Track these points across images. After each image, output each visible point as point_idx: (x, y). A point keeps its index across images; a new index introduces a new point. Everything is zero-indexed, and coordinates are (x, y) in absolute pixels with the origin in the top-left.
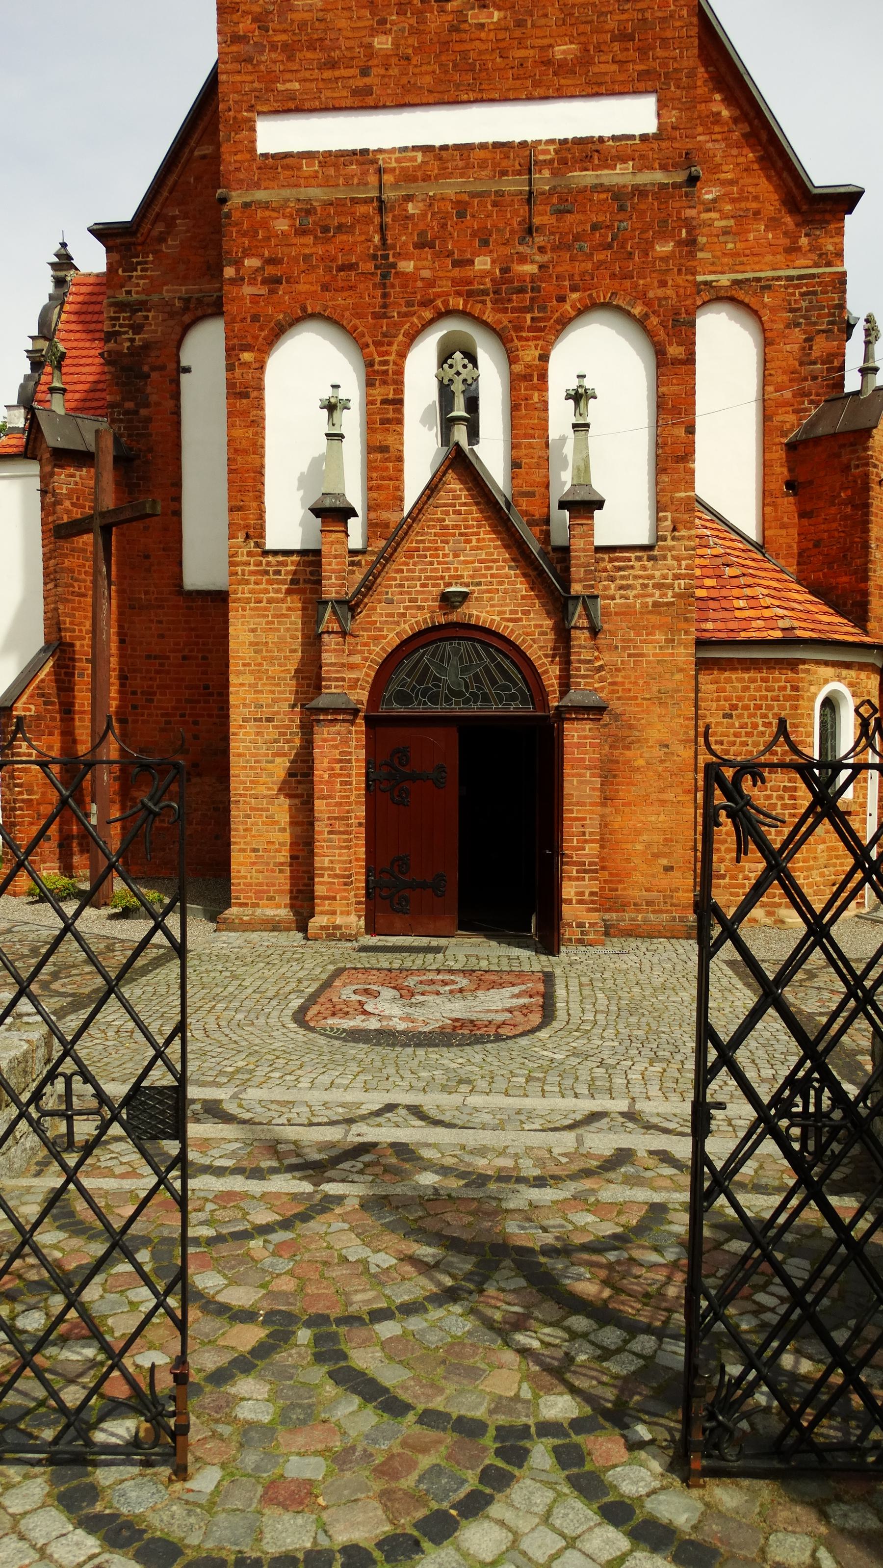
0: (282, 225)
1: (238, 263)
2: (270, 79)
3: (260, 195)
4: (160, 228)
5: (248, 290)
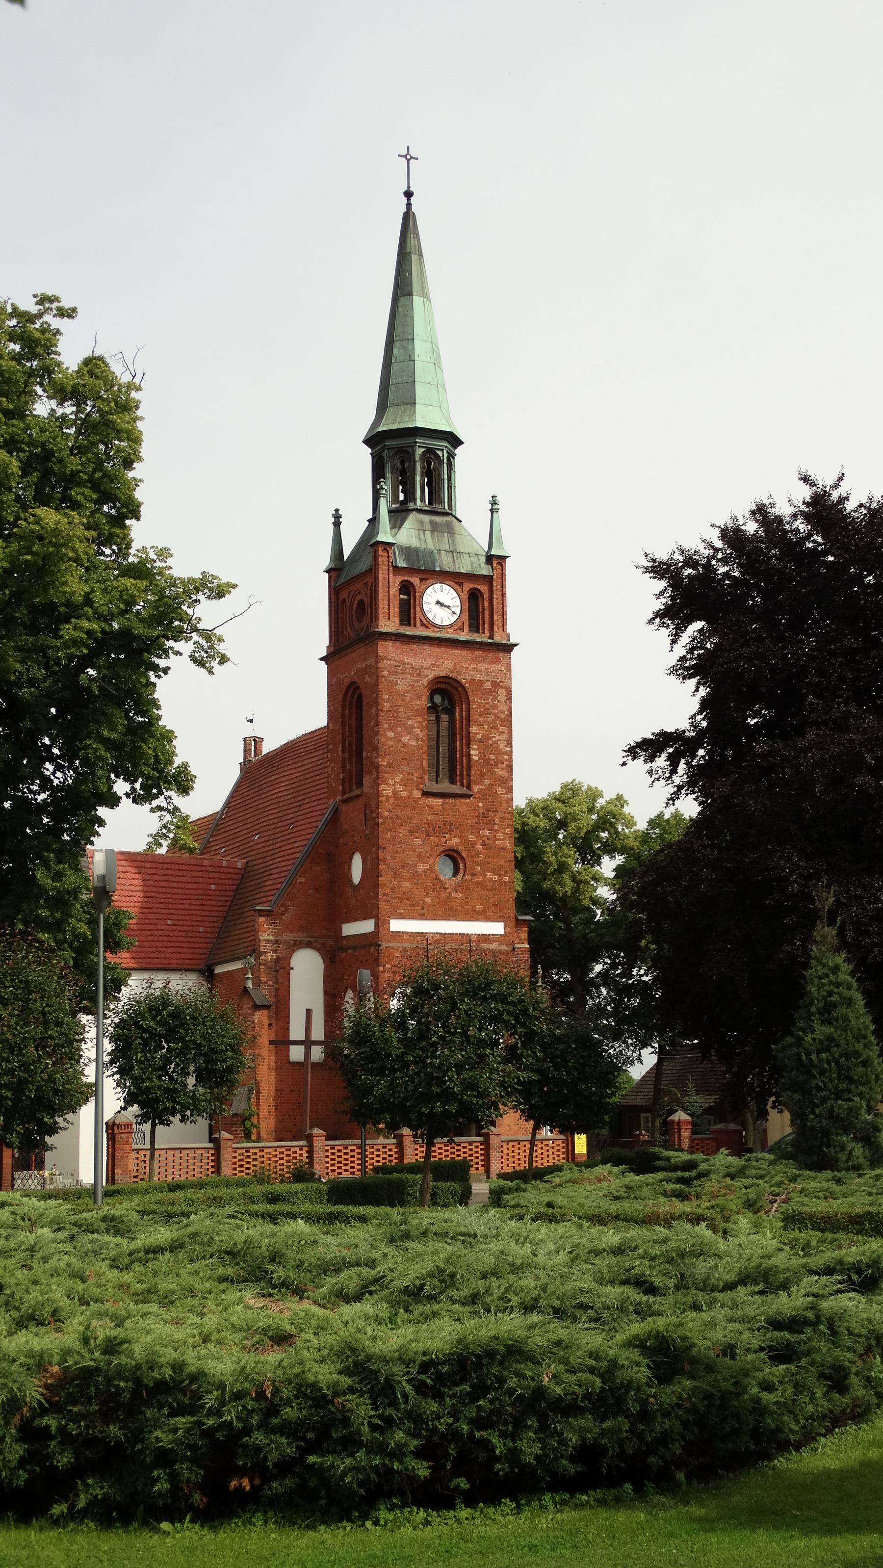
0: (397, 954)
1: (384, 966)
2: (395, 908)
3: (391, 945)
4: (283, 909)
5: (387, 975)
